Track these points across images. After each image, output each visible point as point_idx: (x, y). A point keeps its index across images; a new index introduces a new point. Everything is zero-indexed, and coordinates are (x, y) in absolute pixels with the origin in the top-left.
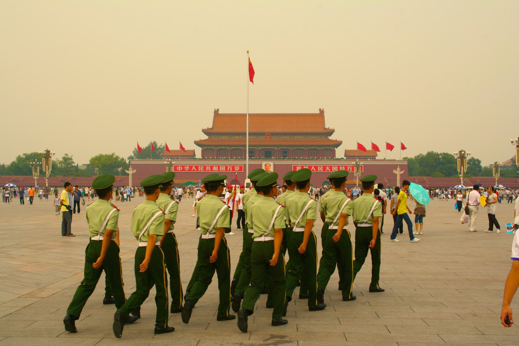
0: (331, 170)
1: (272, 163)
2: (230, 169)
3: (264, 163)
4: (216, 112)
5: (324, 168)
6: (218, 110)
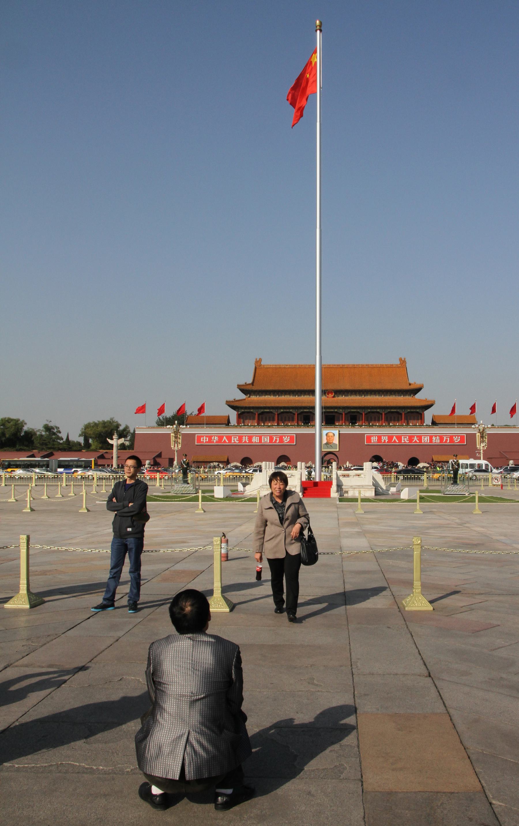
0: (421, 442)
1: (336, 432)
2: (276, 440)
4: (258, 363)
5: (411, 438)
6: (260, 360)
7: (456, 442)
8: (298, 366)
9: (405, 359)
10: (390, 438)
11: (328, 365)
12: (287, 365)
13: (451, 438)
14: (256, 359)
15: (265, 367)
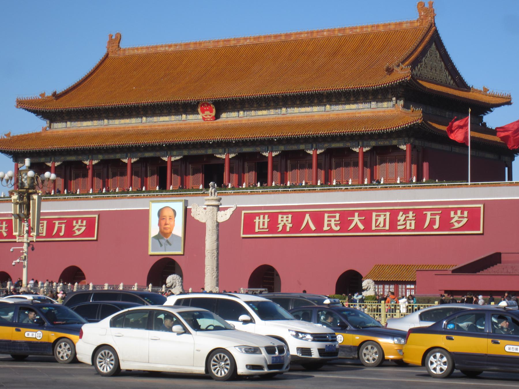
0: (368, 228)
3: (154, 207)
5: (345, 218)
7: (457, 225)
8: (192, 48)
9: (431, 4)
10: (298, 218)
11: (255, 38)
12: (170, 46)
13: (445, 215)
14: (111, 36)
15: (127, 53)
